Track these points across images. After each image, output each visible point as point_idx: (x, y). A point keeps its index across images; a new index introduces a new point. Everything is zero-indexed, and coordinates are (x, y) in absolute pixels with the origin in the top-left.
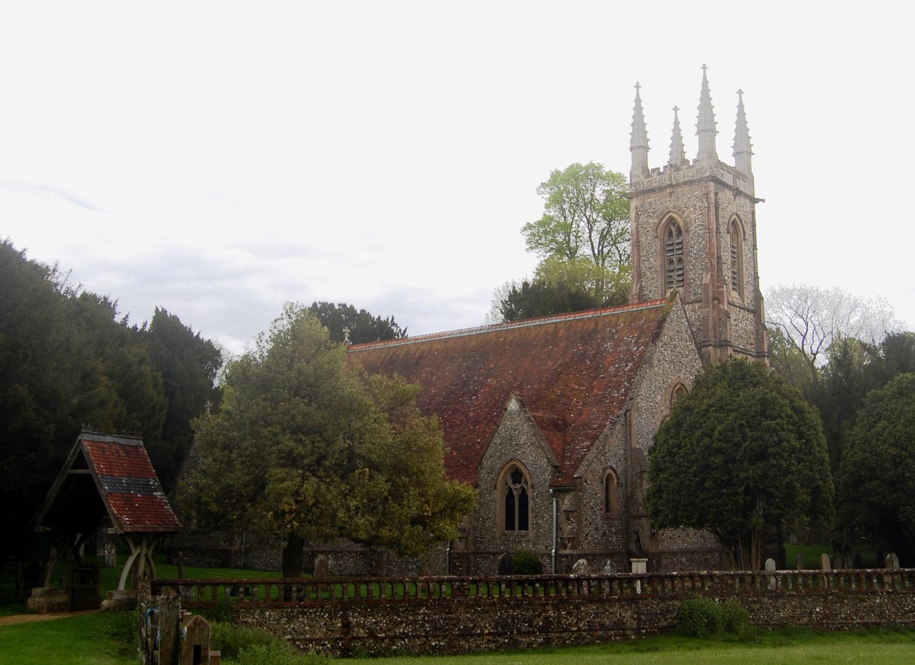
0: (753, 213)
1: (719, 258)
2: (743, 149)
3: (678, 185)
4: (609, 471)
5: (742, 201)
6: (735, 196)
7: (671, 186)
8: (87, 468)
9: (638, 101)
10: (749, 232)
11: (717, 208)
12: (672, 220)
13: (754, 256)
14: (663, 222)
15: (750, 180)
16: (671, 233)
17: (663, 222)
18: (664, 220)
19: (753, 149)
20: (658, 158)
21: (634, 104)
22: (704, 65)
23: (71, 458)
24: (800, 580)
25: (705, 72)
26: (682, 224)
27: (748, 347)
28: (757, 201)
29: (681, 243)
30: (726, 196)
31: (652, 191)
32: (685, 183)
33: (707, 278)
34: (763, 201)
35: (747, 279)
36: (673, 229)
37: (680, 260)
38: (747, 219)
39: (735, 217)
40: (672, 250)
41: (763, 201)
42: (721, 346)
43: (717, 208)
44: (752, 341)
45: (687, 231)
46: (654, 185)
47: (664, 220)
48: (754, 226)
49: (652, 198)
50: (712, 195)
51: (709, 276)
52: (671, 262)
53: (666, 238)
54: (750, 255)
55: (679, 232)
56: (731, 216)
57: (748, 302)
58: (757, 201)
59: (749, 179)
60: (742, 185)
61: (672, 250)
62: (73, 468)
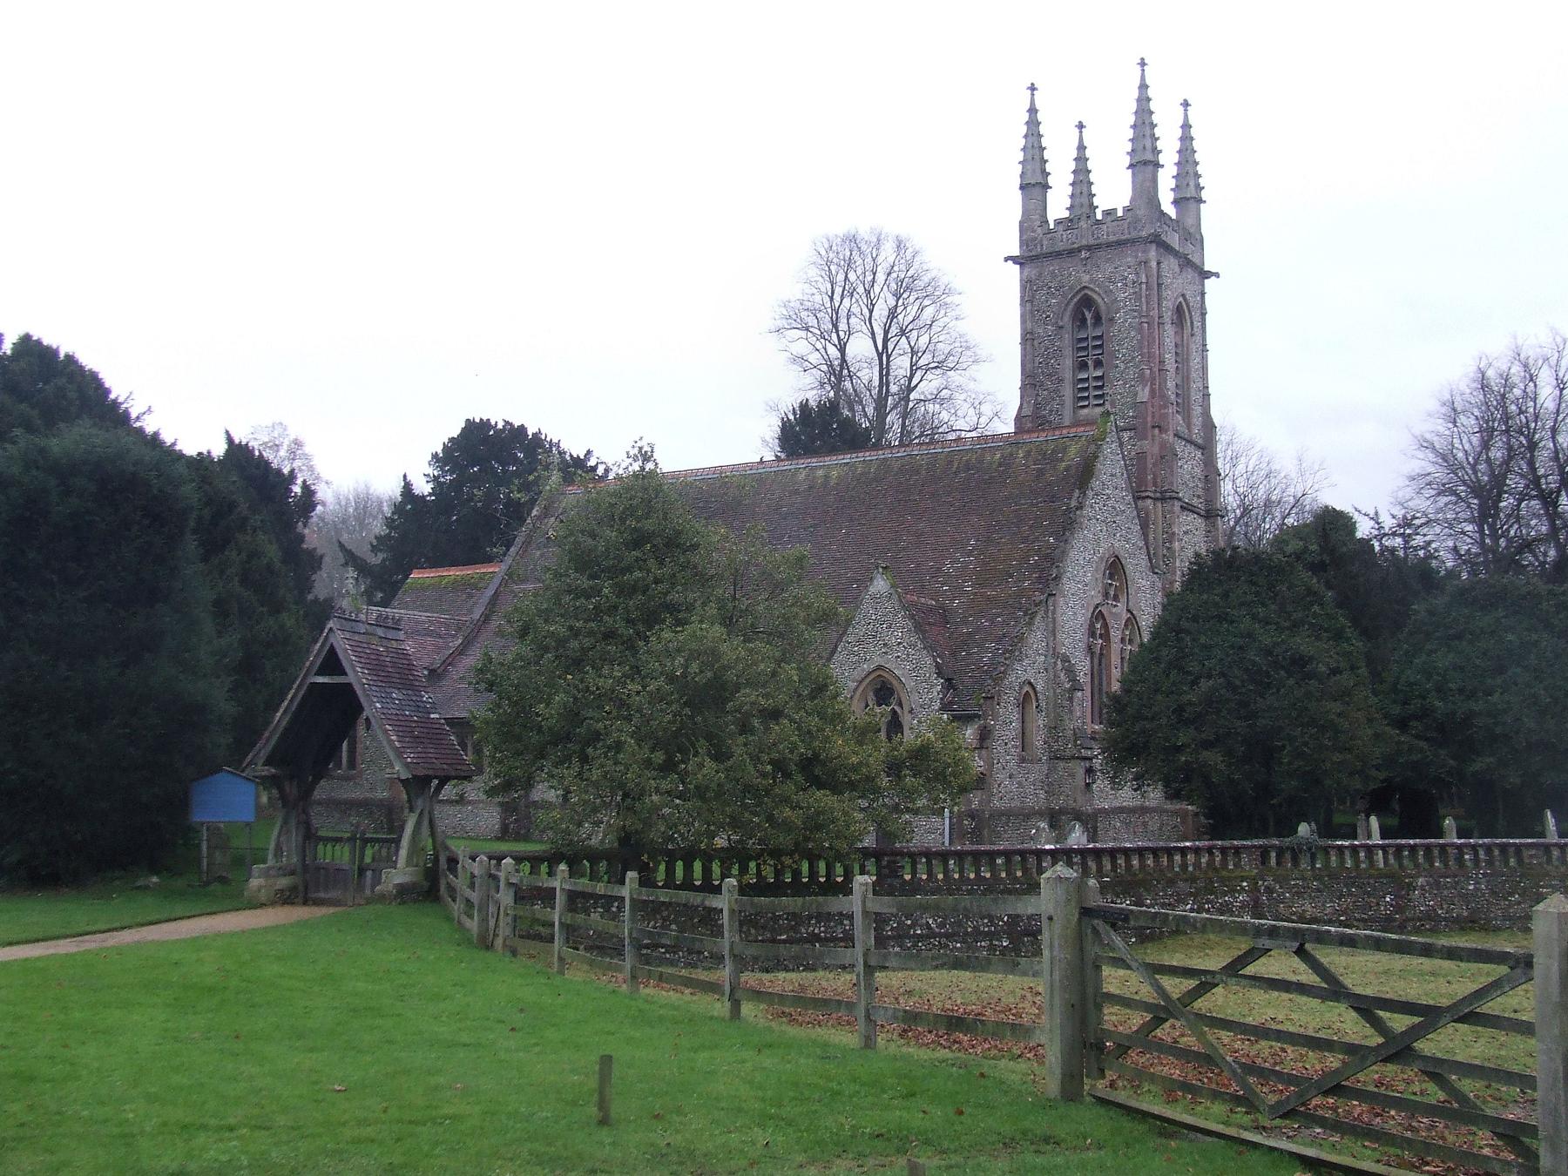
0: (1203, 294)
1: (1162, 362)
2: (1189, 197)
3: (1099, 246)
4: (1027, 688)
5: (1190, 274)
7: (1089, 248)
8: (345, 674)
9: (1033, 110)
10: (1197, 324)
11: (1159, 285)
12: (1087, 302)
13: (1204, 359)
15: (1199, 242)
16: (1084, 320)
19: (1204, 195)
20: (1058, 206)
21: (1026, 117)
24: (1362, 854)
27: (1195, 501)
28: (1208, 275)
29: (1100, 337)
30: (1170, 264)
32: (1109, 245)
33: (1144, 394)
34: (1217, 275)
35: (1196, 396)
36: (1088, 315)
40: (1085, 348)
41: (1217, 275)
42: (1163, 499)
43: (1159, 285)
44: (1200, 492)
45: (1112, 320)
46: (1060, 246)
48: (1203, 314)
49: (1054, 266)
50: (1154, 264)
51: (1147, 390)
55: (1098, 319)
57: (1197, 433)
58: (1208, 275)
59: (1195, 238)
60: (1188, 249)
61: (1085, 348)
62: (318, 674)
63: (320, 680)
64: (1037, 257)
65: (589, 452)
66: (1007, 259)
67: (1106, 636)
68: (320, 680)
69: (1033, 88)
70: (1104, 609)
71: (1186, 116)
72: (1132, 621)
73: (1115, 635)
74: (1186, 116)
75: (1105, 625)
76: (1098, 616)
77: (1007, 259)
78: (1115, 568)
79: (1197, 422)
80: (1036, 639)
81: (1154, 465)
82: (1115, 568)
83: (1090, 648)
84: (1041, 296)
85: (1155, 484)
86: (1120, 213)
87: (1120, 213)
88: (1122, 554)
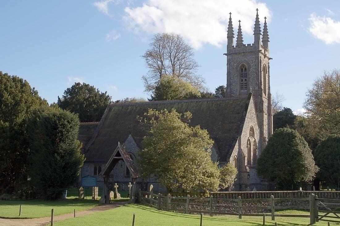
2: (266, 41)
6: (265, 58)
10: (268, 71)
11: (261, 62)
12: (243, 66)
14: (240, 66)
16: (242, 69)
17: (240, 66)
18: (240, 65)
19: (269, 40)
22: (257, 9)
23: (115, 153)
25: (257, 12)
26: (247, 67)
31: (236, 54)
34: (272, 59)
37: (246, 80)
38: (267, 66)
39: (264, 65)
41: (272, 59)
46: (237, 52)
47: (240, 65)
52: (242, 80)
53: (240, 72)
54: (268, 79)
55: (246, 69)
56: (264, 65)
62: (115, 156)
63: (116, 157)
64: (231, 54)
65: (106, 92)
66: (224, 54)
67: (250, 145)
68: (116, 157)
69: (230, 14)
70: (250, 138)
71: (257, 13)
72: (255, 141)
73: (252, 145)
74: (257, 13)
75: (250, 142)
76: (249, 140)
77: (224, 54)
78: (252, 129)
79: (267, 93)
80: (236, 147)
81: (259, 104)
82: (252, 129)
83: (247, 147)
84: (232, 63)
85: (259, 109)
86: (251, 45)
87: (251, 45)
88: (253, 125)
